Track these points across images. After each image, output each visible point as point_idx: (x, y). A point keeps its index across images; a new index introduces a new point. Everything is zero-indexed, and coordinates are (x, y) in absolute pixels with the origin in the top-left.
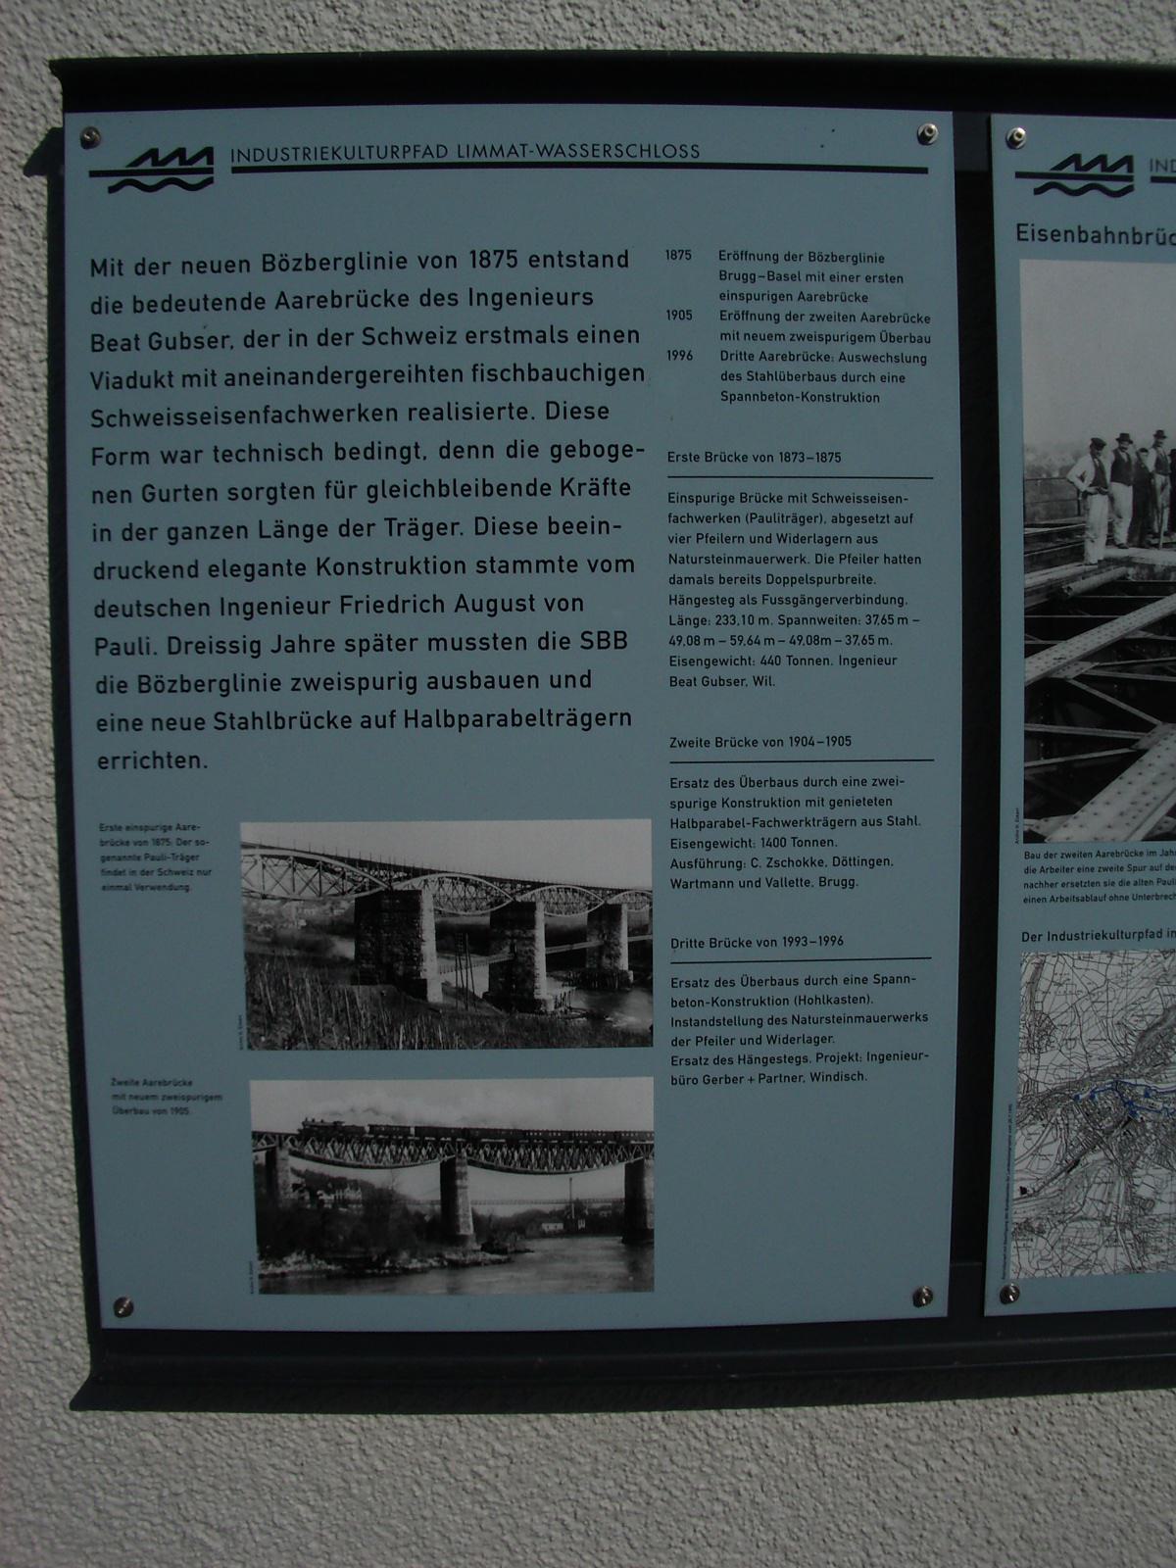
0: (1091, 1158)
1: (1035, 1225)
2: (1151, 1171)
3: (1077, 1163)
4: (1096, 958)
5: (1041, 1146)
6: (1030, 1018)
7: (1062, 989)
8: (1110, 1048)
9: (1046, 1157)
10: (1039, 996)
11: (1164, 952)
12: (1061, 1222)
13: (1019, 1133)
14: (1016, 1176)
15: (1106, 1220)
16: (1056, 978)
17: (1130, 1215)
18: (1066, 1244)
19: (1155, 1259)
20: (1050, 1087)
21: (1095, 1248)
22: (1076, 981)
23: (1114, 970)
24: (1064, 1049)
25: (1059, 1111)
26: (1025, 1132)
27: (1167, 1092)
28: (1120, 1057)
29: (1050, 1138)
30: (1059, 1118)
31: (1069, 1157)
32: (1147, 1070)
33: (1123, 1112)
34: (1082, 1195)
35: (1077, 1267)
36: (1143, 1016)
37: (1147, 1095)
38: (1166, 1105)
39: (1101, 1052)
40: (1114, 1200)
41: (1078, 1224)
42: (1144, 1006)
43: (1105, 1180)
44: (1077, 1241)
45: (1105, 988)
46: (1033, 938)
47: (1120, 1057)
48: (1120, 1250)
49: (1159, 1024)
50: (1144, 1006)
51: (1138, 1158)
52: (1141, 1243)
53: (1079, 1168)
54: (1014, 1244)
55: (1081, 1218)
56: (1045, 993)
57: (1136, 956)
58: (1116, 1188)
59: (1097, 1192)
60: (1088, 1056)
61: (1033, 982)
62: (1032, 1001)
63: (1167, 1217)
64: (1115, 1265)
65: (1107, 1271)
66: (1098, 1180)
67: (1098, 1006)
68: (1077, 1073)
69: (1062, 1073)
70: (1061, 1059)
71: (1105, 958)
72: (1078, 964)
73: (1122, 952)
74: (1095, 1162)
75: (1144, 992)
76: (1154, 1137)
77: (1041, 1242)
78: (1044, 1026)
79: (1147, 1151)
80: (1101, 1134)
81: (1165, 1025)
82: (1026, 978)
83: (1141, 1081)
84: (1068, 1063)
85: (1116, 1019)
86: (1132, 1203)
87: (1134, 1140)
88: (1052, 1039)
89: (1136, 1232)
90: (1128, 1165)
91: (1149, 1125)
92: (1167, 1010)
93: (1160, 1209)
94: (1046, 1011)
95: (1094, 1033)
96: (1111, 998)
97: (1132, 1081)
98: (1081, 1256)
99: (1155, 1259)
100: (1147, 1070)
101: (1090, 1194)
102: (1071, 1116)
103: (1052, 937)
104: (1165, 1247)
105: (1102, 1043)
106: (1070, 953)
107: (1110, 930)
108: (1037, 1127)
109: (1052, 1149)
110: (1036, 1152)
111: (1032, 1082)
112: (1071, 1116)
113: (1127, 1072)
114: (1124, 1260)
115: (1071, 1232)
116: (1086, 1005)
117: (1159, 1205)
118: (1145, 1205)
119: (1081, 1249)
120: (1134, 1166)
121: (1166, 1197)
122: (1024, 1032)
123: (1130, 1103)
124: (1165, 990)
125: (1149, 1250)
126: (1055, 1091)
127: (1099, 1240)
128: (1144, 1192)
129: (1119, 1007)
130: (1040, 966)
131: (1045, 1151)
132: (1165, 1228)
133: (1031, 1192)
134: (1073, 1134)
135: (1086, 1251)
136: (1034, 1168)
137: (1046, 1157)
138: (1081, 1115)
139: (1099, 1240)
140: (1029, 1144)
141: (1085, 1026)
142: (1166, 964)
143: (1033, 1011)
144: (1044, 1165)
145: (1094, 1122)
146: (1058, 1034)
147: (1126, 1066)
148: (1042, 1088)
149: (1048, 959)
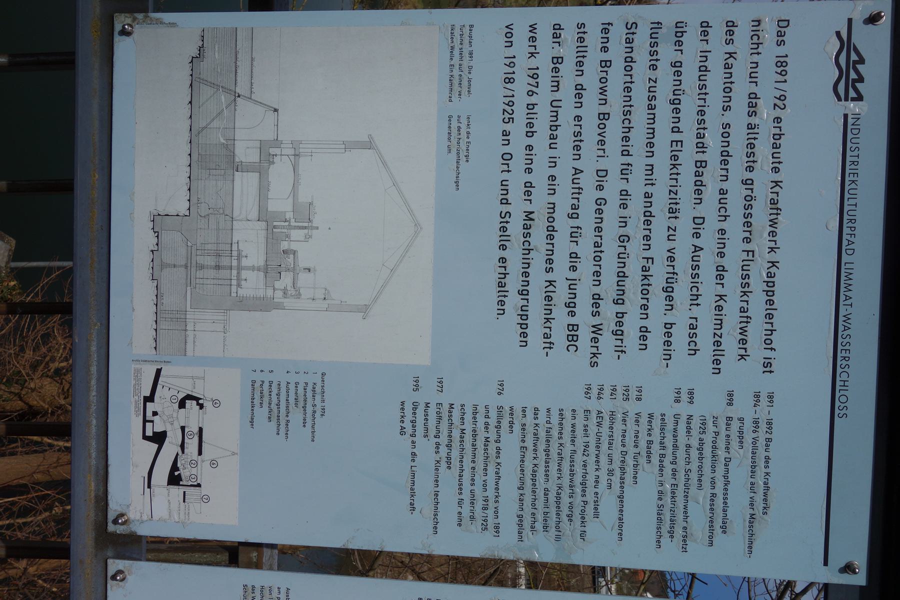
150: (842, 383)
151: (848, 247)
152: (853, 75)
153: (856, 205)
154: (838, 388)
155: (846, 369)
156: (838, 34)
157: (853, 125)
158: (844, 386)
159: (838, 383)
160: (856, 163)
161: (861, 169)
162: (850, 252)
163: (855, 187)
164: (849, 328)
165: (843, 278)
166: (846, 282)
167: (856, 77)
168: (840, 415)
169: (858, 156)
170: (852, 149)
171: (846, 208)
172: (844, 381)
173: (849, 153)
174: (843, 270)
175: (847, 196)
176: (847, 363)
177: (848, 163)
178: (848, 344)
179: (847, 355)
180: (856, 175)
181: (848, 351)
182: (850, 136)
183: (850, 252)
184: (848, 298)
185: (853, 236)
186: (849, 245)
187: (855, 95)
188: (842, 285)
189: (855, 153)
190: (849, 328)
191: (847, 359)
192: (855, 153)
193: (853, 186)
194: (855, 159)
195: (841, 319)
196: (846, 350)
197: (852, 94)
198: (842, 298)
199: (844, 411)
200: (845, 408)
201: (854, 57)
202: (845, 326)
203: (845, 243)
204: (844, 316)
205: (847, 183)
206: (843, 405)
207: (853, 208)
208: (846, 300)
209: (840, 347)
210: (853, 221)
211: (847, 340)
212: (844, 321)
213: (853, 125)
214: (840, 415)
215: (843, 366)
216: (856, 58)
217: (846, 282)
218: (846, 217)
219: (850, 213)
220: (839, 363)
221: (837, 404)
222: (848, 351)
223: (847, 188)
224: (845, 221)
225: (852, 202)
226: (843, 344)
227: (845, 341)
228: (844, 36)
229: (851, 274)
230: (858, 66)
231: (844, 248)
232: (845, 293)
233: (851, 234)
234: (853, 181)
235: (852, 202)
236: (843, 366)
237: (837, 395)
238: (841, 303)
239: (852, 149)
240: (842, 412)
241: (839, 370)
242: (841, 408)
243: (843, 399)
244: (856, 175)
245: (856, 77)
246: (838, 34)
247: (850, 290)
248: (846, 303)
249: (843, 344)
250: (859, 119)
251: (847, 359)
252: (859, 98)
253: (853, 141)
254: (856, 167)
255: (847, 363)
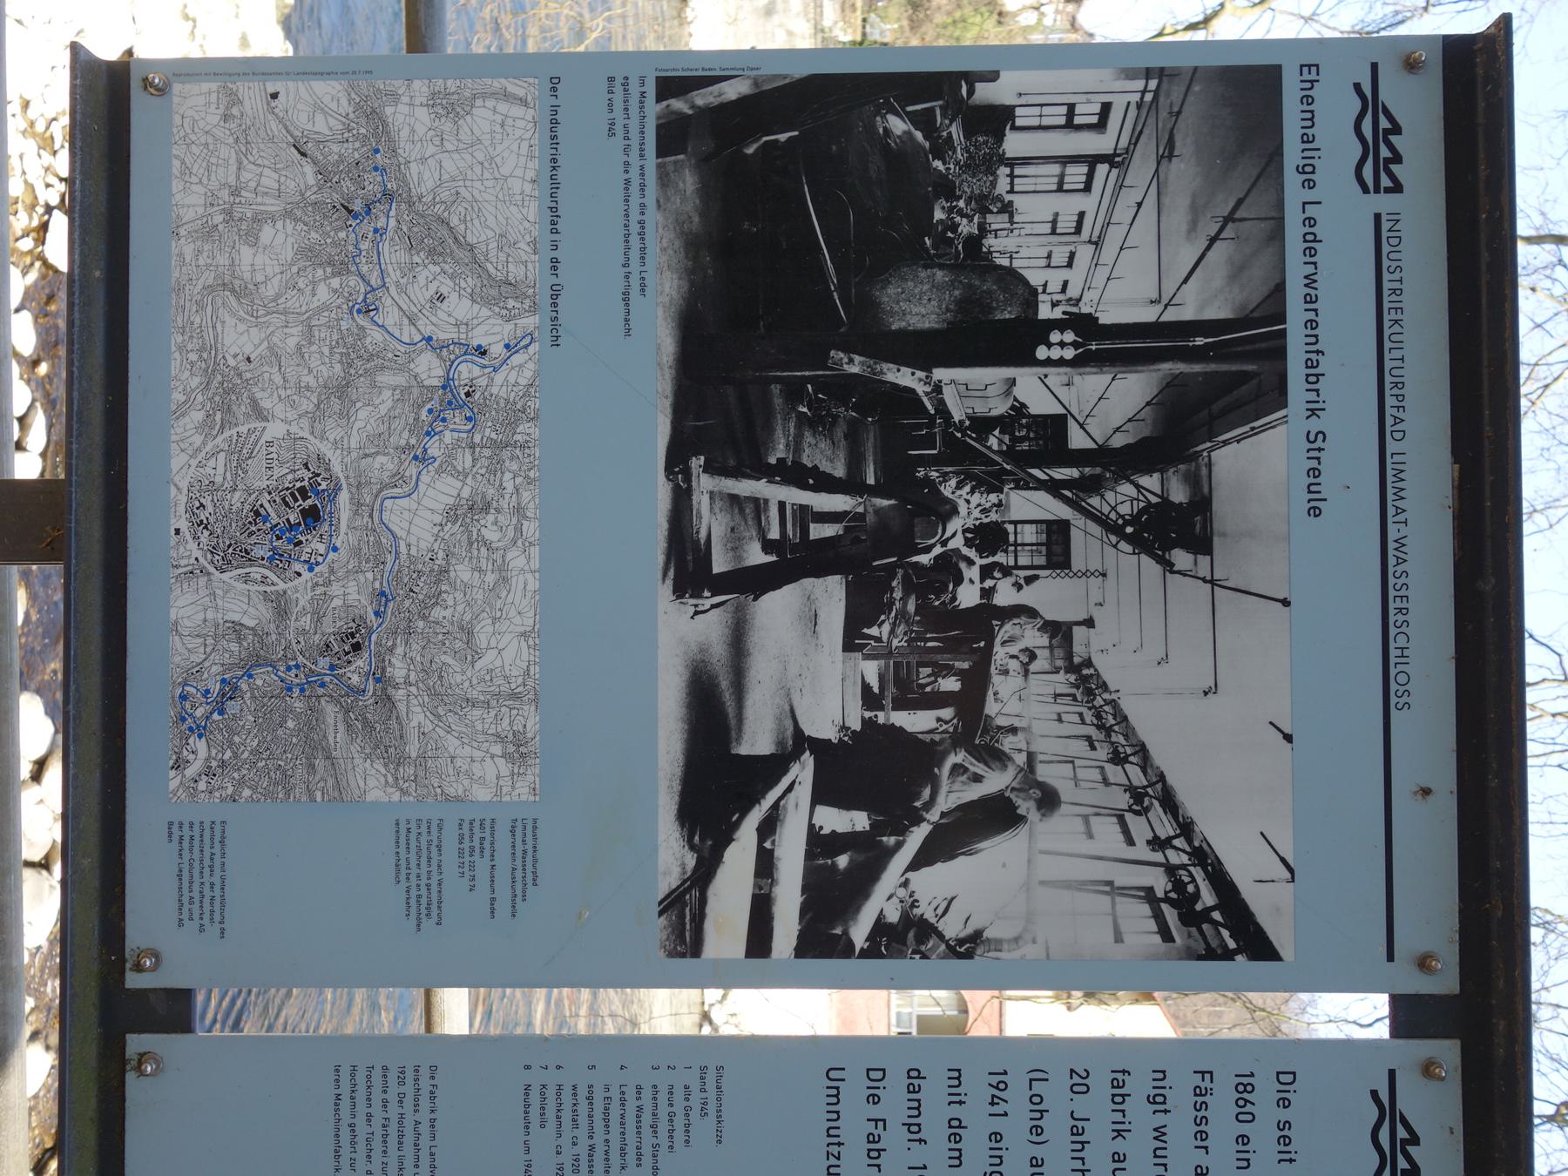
0: (309, 170)
1: (235, 111)
2: (291, 240)
3: (304, 154)
4: (530, 165)
5: (325, 113)
6: (467, 94)
7: (498, 128)
8: (430, 184)
9: (311, 119)
10: (490, 103)
11: (534, 242)
12: (237, 140)
13: (340, 88)
14: (291, 84)
15: (235, 192)
16: (509, 122)
17: (241, 219)
18: (211, 147)
19: (188, 251)
20: (390, 120)
21: (205, 181)
22: (506, 144)
23: (516, 185)
24: (432, 133)
25: (363, 131)
26: (340, 95)
27: (379, 253)
28: (420, 197)
29: (332, 122)
30: (355, 132)
31: (310, 145)
32: (405, 229)
33: (357, 206)
34: (267, 163)
35: (183, 162)
36: (465, 221)
37: (376, 231)
38: (364, 253)
39: (427, 175)
40: (259, 199)
41: (233, 160)
42: (476, 222)
43: (283, 187)
44: (213, 160)
45: (498, 176)
46: (554, 89)
47: (420, 197)
48: (201, 210)
49: (456, 238)
50: (476, 222)
51: (306, 225)
52: (209, 232)
53: (299, 156)
54: (214, 86)
55: (240, 163)
56: (494, 111)
57: (532, 210)
58: (273, 201)
59: (270, 180)
60: (423, 160)
61: (506, 96)
62: (484, 96)
63: (237, 262)
64: (183, 206)
65: (178, 197)
66: (283, 179)
67: (478, 169)
68: (405, 149)
69: (405, 133)
70: (421, 130)
71: (530, 174)
72: (525, 145)
73: (537, 194)
74: (304, 175)
75: (491, 221)
76: (329, 241)
77: (214, 119)
78: (458, 110)
79: (313, 235)
80: (334, 180)
81: (454, 247)
82: (511, 89)
83: (392, 222)
84: (416, 138)
85: (462, 191)
86: (255, 220)
87: (325, 217)
88: (443, 119)
89: (220, 227)
90: (299, 213)
91: (342, 235)
92: (472, 248)
93: (246, 253)
94: (475, 111)
95: (449, 166)
96: (485, 182)
97: (392, 213)
98: (196, 167)
99: (188, 251)
100: (405, 229)
101: (267, 172)
102: (357, 145)
103: (555, 110)
104: (201, 262)
105: (437, 176)
106: (536, 135)
107: (561, 175)
108: (346, 108)
109: (321, 125)
110: (318, 107)
111: (395, 97)
112: (357, 145)
113: (403, 206)
114: (189, 215)
115: (224, 152)
116: (480, 156)
117: (252, 251)
118: (252, 238)
119: (204, 165)
120: (296, 220)
121: (259, 260)
122: (452, 85)
123: (368, 213)
124: (493, 245)
125: (199, 243)
126: (385, 124)
127: (214, 185)
128: (267, 233)
129: (476, 193)
130: (523, 102)
131: (319, 117)
132: (222, 260)
133: (273, 104)
134: (335, 148)
135: (202, 171)
136: (300, 106)
137: (311, 119)
138: (357, 156)
139: (214, 185)
140: (327, 100)
141: (455, 156)
142: (522, 245)
143: (474, 97)
144: (303, 117)
145: (349, 171)
146: (448, 126)
147: (411, 204)
148: (389, 111)
149: (531, 111)
150: (1399, 652)
151: (1397, 428)
152: (1385, 152)
153: (1402, 359)
154: (1393, 660)
155: (1404, 629)
156: (1357, 87)
157: (1389, 231)
158: (1402, 656)
159: (1393, 653)
160: (1398, 292)
161: (1407, 300)
162: (1398, 436)
163: (1400, 330)
164: (1405, 561)
165: (1390, 479)
166: (1395, 485)
167: (1390, 155)
168: (1399, 706)
169: (1401, 281)
170: (1391, 270)
171: (1388, 365)
172: (1402, 649)
173: (1386, 276)
174: (1389, 466)
175: (1387, 345)
176: (1404, 618)
177: (1386, 293)
178: (1405, 587)
179: (1404, 605)
180: (1399, 311)
181: (1404, 599)
182: (1385, 249)
183: (1398, 436)
184: (1399, 511)
185: (1401, 409)
186: (1395, 424)
187: (1390, 184)
188: (1390, 491)
189: (1396, 276)
190: (1405, 561)
191: (1404, 611)
192: (1396, 276)
193: (1397, 328)
194: (1397, 285)
195: (1391, 545)
196: (1402, 597)
197: (1385, 182)
198: (1391, 511)
199: (1405, 699)
200: (1406, 693)
201: (1384, 123)
202: (1398, 558)
203: (1389, 421)
204: (1396, 541)
205: (1387, 324)
206: (1402, 689)
207: (1399, 363)
208: (1397, 514)
209: (1392, 593)
210: (1400, 386)
211: (1403, 580)
212: (1396, 549)
213: (1389, 231)
214: (1399, 706)
215: (1398, 624)
216: (1389, 126)
217: (1395, 485)
218: (1388, 379)
219: (1395, 372)
220: (1392, 619)
221: (1393, 687)
222: (1404, 599)
223: (1387, 332)
224: (1388, 386)
225: (1397, 354)
226: (1398, 587)
227: (1400, 582)
228: (1367, 89)
229: (1402, 471)
230: (1393, 138)
231: (1388, 429)
232: (1395, 503)
233: (1398, 407)
234: (1396, 321)
235: (1397, 354)
236: (1398, 624)
237: (1393, 672)
238: (1390, 520)
239: (1391, 270)
240: (1402, 701)
241: (1393, 631)
242: (1399, 694)
243: (1402, 678)
244: (1399, 311)
245: (1390, 155)
246: (1357, 87)
247: (1403, 498)
248: (1397, 519)
249: (1398, 587)
250: (1398, 221)
251: (1404, 611)
252: (1397, 188)
253: (1392, 256)
254: (1398, 299)
255: (1404, 618)
